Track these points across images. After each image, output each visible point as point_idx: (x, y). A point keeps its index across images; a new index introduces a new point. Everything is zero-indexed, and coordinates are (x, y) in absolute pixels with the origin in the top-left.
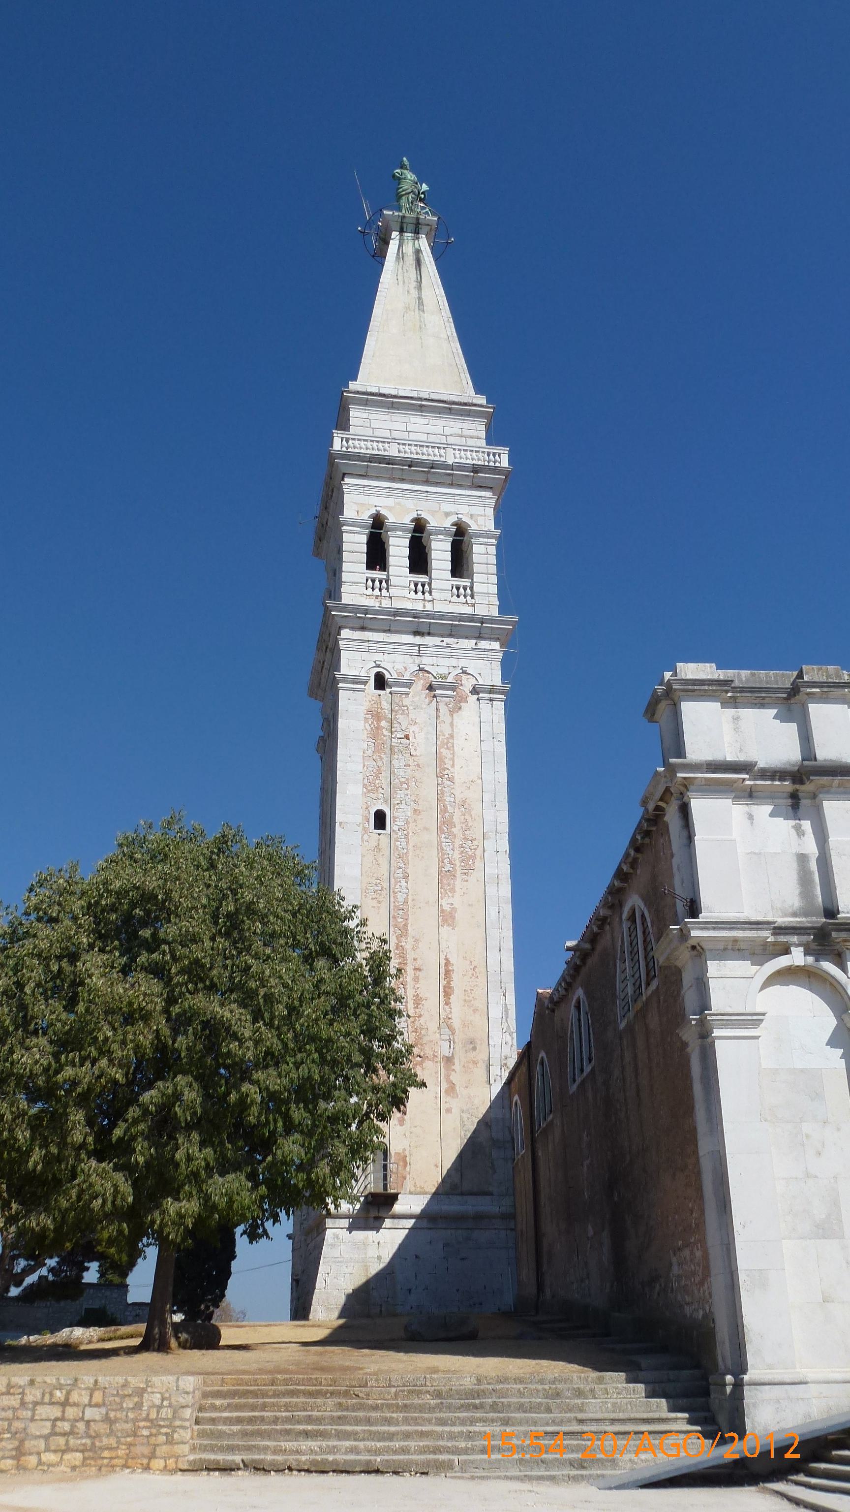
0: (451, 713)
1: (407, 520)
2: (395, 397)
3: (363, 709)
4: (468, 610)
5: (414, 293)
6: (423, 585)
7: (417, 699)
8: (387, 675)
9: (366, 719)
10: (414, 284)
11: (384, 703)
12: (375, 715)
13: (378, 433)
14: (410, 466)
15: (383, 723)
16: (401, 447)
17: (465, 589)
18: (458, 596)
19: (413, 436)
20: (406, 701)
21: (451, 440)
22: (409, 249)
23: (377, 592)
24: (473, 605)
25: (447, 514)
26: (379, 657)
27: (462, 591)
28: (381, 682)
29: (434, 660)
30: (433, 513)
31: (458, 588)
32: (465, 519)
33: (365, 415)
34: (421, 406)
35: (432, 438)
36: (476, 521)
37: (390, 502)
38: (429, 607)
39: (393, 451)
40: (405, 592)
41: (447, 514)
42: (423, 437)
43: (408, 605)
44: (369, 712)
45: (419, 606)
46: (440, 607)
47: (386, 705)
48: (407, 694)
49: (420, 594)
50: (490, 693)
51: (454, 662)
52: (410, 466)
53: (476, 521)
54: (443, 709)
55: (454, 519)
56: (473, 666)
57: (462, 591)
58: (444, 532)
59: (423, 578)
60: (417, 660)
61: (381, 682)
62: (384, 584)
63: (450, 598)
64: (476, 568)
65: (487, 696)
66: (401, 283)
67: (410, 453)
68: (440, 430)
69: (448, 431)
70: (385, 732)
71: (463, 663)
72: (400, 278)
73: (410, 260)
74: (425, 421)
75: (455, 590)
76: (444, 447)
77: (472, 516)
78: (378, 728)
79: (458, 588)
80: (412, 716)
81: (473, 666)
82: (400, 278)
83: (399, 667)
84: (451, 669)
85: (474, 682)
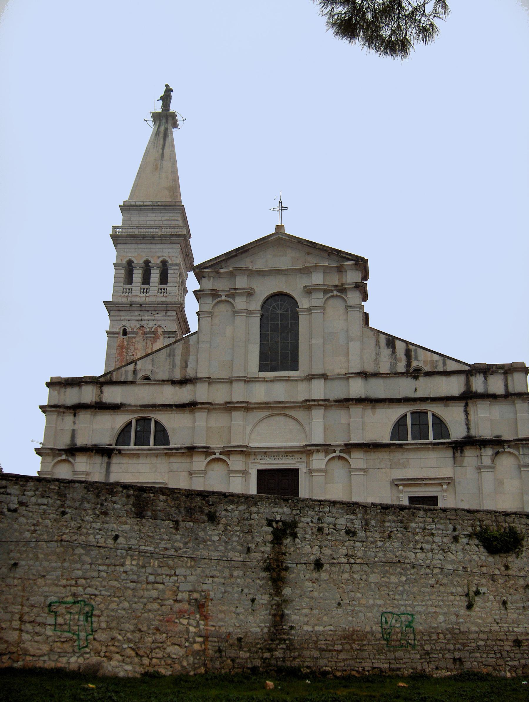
0: (152, 344)
1: (141, 262)
2: (140, 206)
3: (116, 345)
4: (163, 299)
5: (160, 151)
6: (147, 289)
7: (138, 339)
8: (128, 330)
9: (117, 349)
10: (161, 146)
11: (125, 342)
12: (121, 347)
13: (134, 223)
14: (143, 238)
15: (124, 350)
16: (140, 230)
17: (164, 289)
18: (161, 293)
19: (148, 223)
20: (134, 340)
21: (165, 223)
22: (162, 129)
23: (127, 294)
24: (166, 297)
25: (159, 257)
26: (124, 323)
27: (163, 290)
28: (125, 333)
29: (147, 322)
30: (153, 257)
31: (161, 289)
32: (167, 259)
33: (129, 216)
34: (152, 209)
35: (157, 223)
36: (171, 259)
37: (136, 254)
38: (148, 300)
39: (136, 232)
40: (138, 294)
41: (159, 257)
42: (152, 223)
43: (138, 300)
44: (119, 346)
45: (143, 300)
46: (152, 299)
47: (126, 342)
48: (135, 337)
49: (145, 293)
50: (169, 334)
51: (155, 322)
52: (143, 238)
53: (171, 259)
54: (149, 343)
55: (161, 259)
56: (162, 323)
57: (163, 290)
58: (157, 265)
59: (146, 287)
60: (140, 323)
61: (125, 333)
62: (130, 290)
63: (157, 294)
64: (169, 280)
65: (168, 336)
66: (155, 147)
67: (143, 231)
68: (160, 218)
69: (164, 219)
70: (125, 354)
71: (159, 322)
72: (155, 145)
73: (162, 135)
74: (154, 215)
75: (160, 290)
76: (160, 227)
77: (169, 257)
78: (123, 352)
79: (161, 289)
80: (136, 346)
81: (162, 323)
82: (155, 145)
83: (133, 326)
84: (154, 325)
85: (162, 330)
